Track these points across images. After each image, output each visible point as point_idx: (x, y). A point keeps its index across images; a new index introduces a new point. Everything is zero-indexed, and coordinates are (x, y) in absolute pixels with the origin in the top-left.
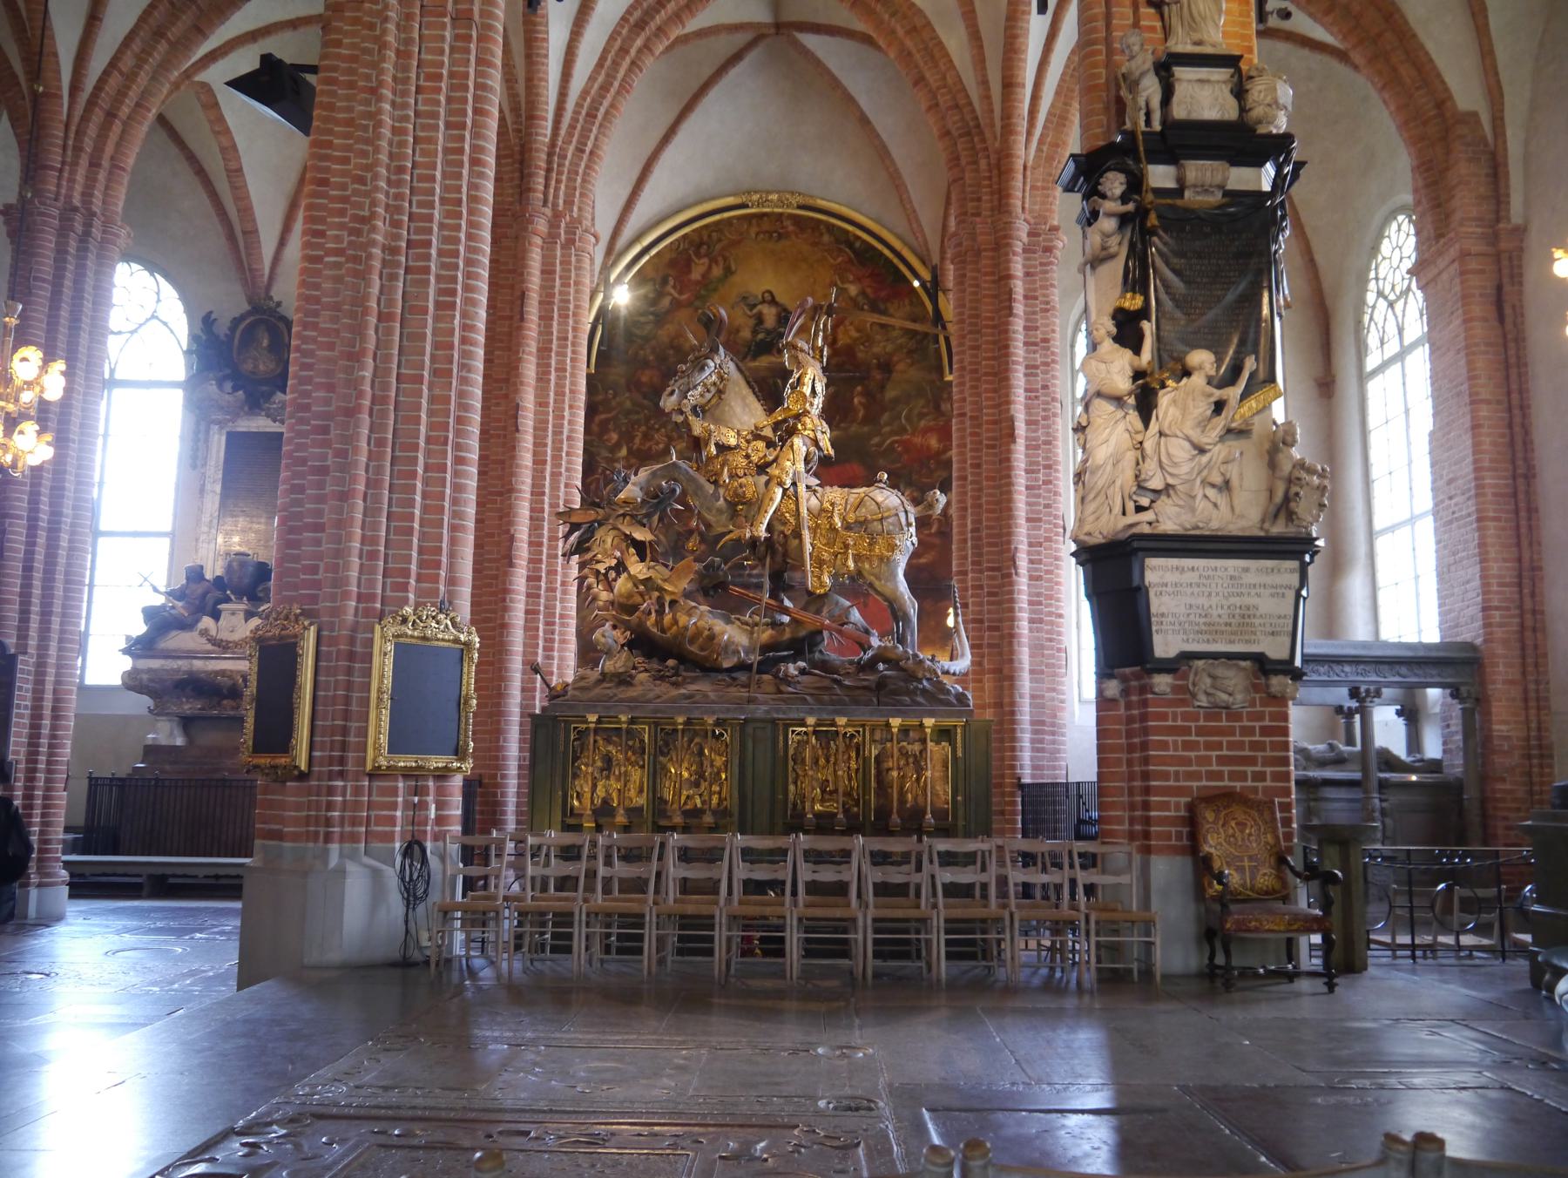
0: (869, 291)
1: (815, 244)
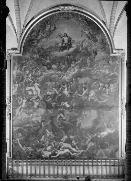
0: (91, 32)
1: (77, 20)
